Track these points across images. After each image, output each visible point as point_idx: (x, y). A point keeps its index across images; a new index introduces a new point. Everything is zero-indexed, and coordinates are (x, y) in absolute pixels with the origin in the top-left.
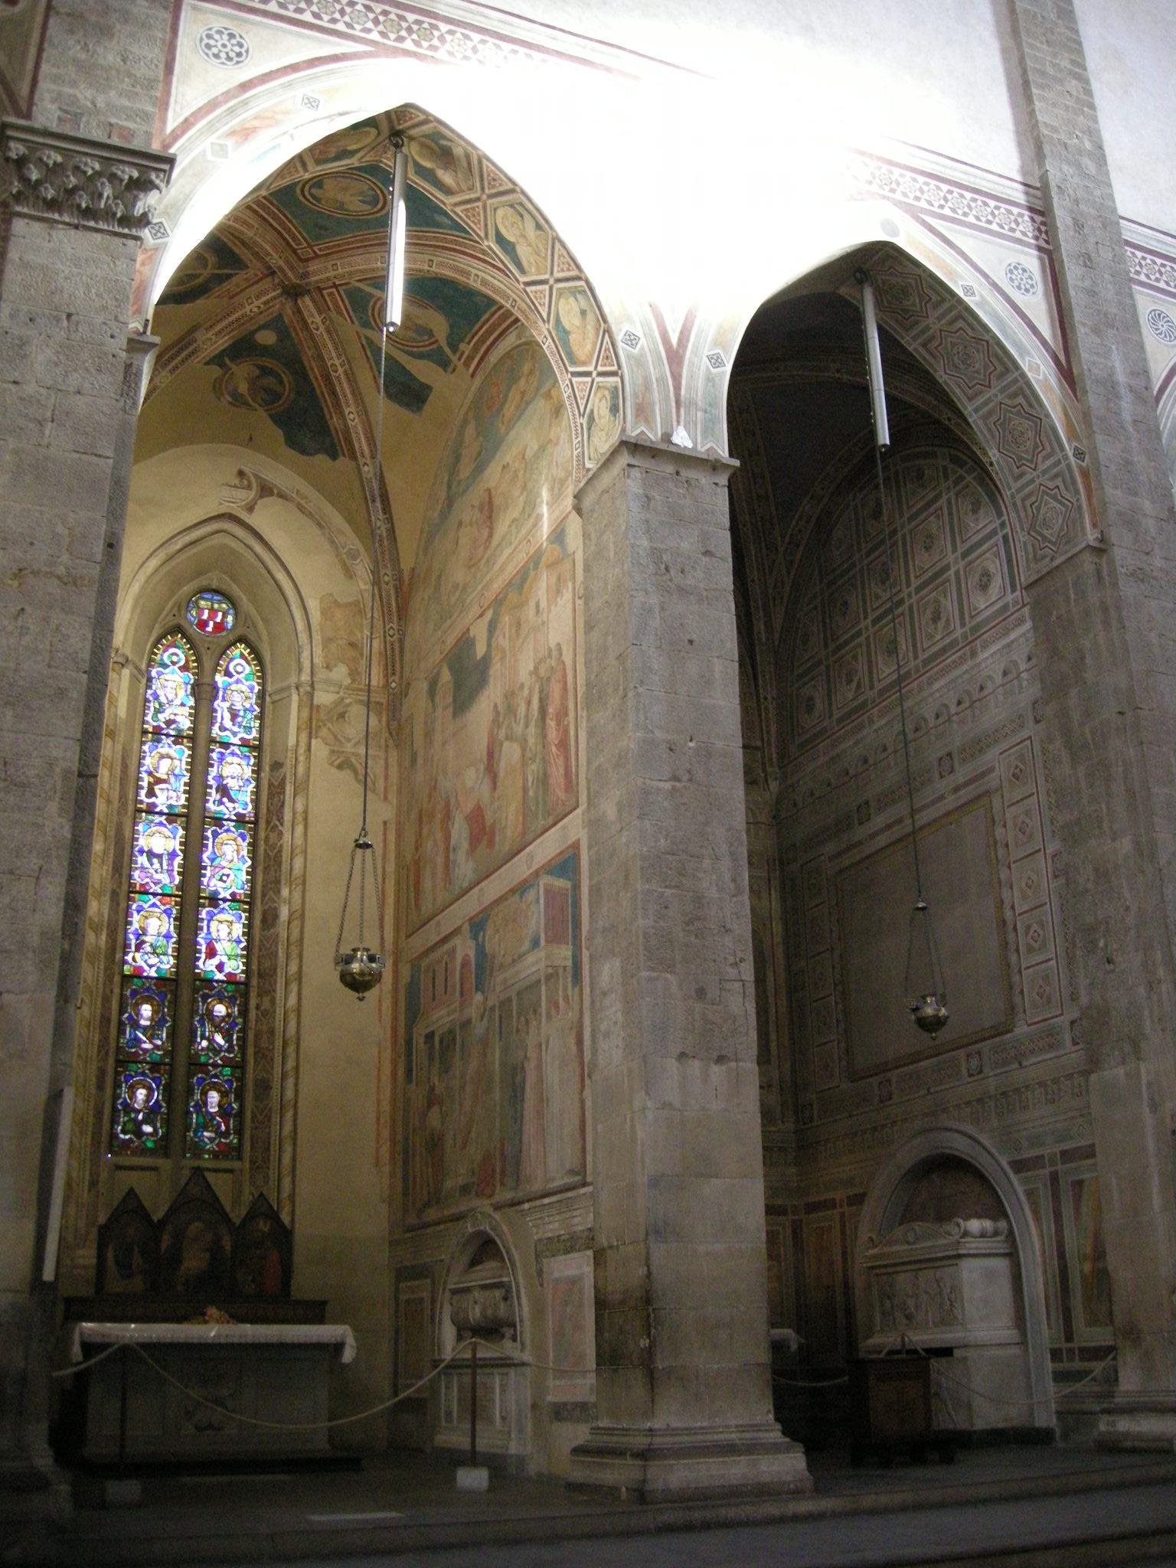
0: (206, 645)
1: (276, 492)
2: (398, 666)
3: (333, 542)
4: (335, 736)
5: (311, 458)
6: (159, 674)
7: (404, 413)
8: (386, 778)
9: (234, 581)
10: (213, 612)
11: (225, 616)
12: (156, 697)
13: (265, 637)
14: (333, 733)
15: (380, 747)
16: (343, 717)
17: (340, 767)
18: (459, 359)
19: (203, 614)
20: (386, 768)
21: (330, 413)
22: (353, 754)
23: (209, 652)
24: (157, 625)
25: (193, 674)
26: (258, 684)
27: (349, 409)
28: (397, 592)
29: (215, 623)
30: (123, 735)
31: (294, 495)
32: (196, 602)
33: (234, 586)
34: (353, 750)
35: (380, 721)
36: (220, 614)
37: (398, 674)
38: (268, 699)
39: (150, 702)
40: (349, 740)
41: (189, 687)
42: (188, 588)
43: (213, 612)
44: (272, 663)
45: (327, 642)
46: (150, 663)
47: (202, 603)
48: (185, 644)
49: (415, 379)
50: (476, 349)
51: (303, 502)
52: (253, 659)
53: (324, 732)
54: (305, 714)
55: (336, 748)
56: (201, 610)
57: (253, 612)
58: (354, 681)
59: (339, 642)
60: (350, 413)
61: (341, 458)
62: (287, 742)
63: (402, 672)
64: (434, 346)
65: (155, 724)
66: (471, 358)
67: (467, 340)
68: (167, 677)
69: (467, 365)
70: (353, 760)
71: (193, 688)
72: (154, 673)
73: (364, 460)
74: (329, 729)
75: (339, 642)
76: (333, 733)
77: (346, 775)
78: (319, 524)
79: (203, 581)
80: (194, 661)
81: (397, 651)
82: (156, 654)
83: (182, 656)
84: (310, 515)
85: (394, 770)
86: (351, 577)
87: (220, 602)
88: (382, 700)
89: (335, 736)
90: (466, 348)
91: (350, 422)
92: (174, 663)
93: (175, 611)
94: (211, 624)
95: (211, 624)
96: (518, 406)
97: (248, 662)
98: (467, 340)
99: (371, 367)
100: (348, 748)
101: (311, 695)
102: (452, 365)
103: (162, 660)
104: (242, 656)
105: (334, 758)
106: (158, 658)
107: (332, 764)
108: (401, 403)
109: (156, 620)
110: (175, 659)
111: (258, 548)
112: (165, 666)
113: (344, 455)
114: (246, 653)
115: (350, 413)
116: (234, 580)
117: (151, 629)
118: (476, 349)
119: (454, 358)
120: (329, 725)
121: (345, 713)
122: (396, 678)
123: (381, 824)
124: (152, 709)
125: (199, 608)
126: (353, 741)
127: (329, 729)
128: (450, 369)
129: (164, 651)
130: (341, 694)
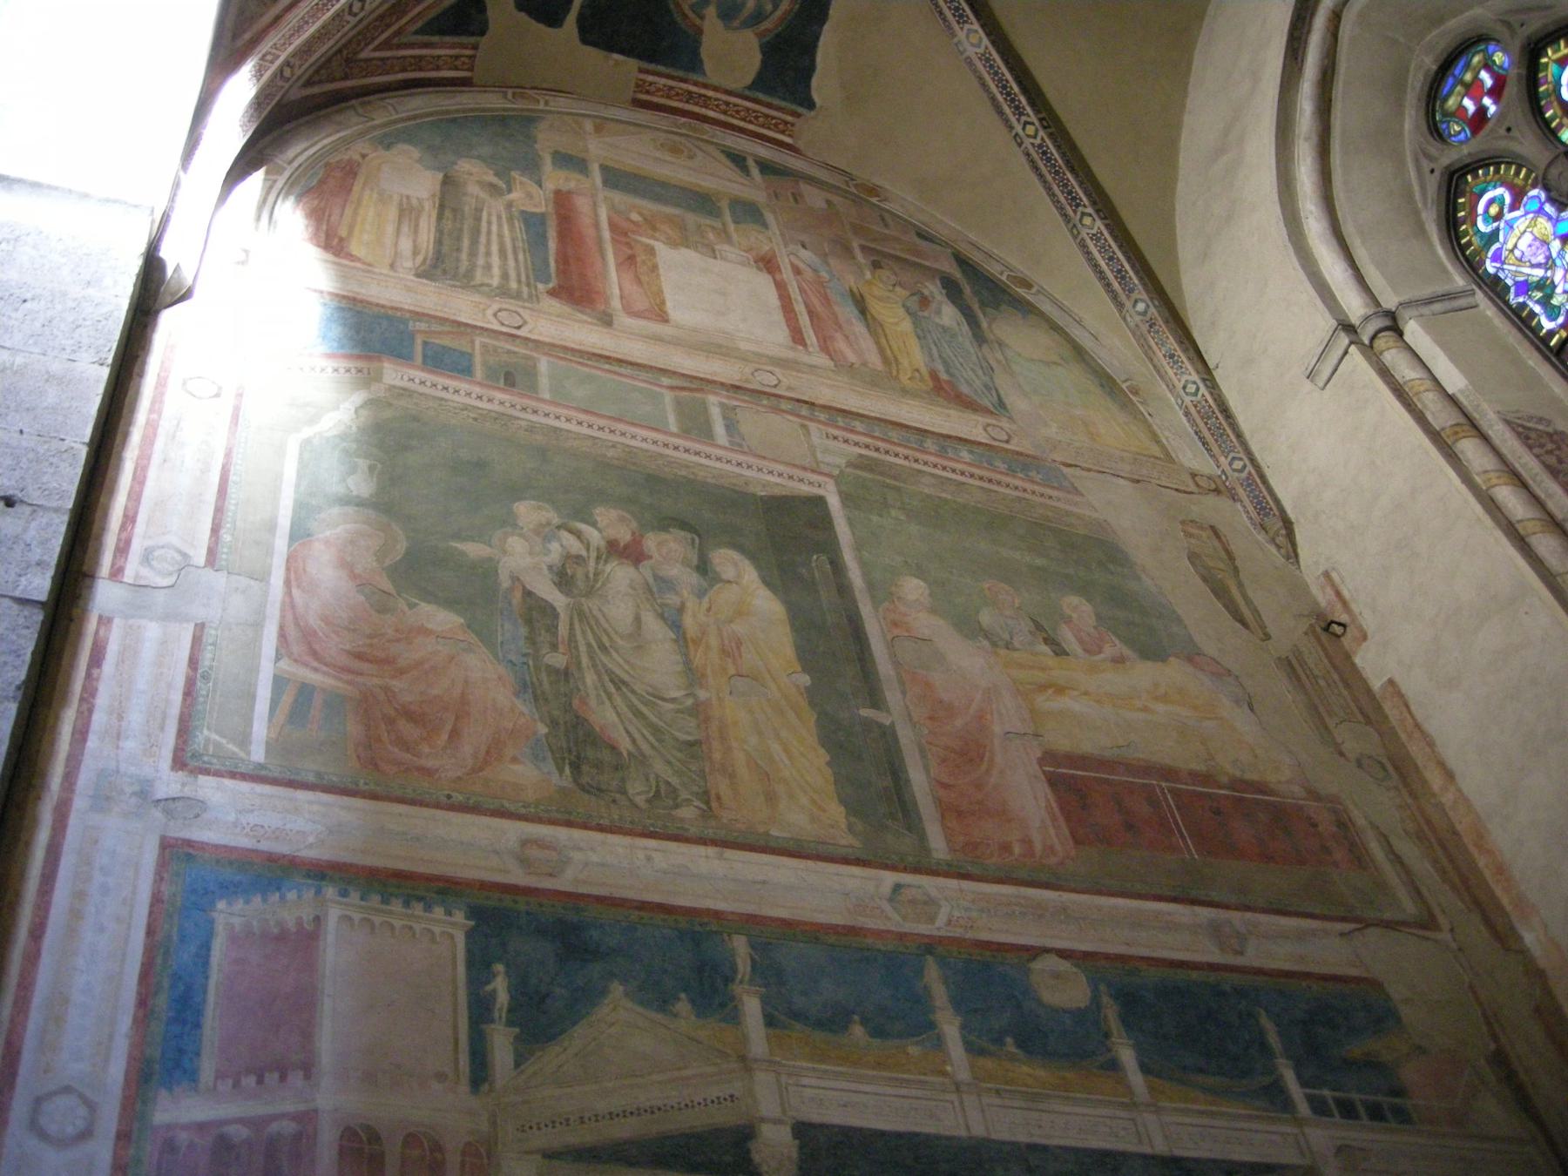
0: (1502, 132)
6: (1497, 257)
9: (1441, 20)
11: (1488, 66)
12: (1524, 287)
19: (1465, 109)
23: (1515, 133)
24: (1424, 215)
25: (1534, 186)
30: (1485, 406)
32: (1446, 114)
33: (1452, 23)
36: (1485, 76)
39: (1524, 305)
41: (1548, 208)
42: (1411, 120)
43: (1473, 89)
46: (1472, 265)
47: (1451, 103)
48: (1486, 174)
65: (1561, 320)
68: (1510, 246)
71: (1550, 200)
72: (1490, 267)
79: (1416, 83)
80: (1517, 173)
82: (1469, 244)
83: (1500, 191)
87: (1467, 66)
92: (1499, 217)
93: (1426, 165)
94: (1487, 101)
95: (1487, 101)
103: (1482, 235)
106: (1476, 241)
109: (1417, 213)
110: (1494, 210)
112: (1494, 235)
116: (1437, 20)
117: (1421, 230)
124: (1537, 309)
129: (1474, 224)
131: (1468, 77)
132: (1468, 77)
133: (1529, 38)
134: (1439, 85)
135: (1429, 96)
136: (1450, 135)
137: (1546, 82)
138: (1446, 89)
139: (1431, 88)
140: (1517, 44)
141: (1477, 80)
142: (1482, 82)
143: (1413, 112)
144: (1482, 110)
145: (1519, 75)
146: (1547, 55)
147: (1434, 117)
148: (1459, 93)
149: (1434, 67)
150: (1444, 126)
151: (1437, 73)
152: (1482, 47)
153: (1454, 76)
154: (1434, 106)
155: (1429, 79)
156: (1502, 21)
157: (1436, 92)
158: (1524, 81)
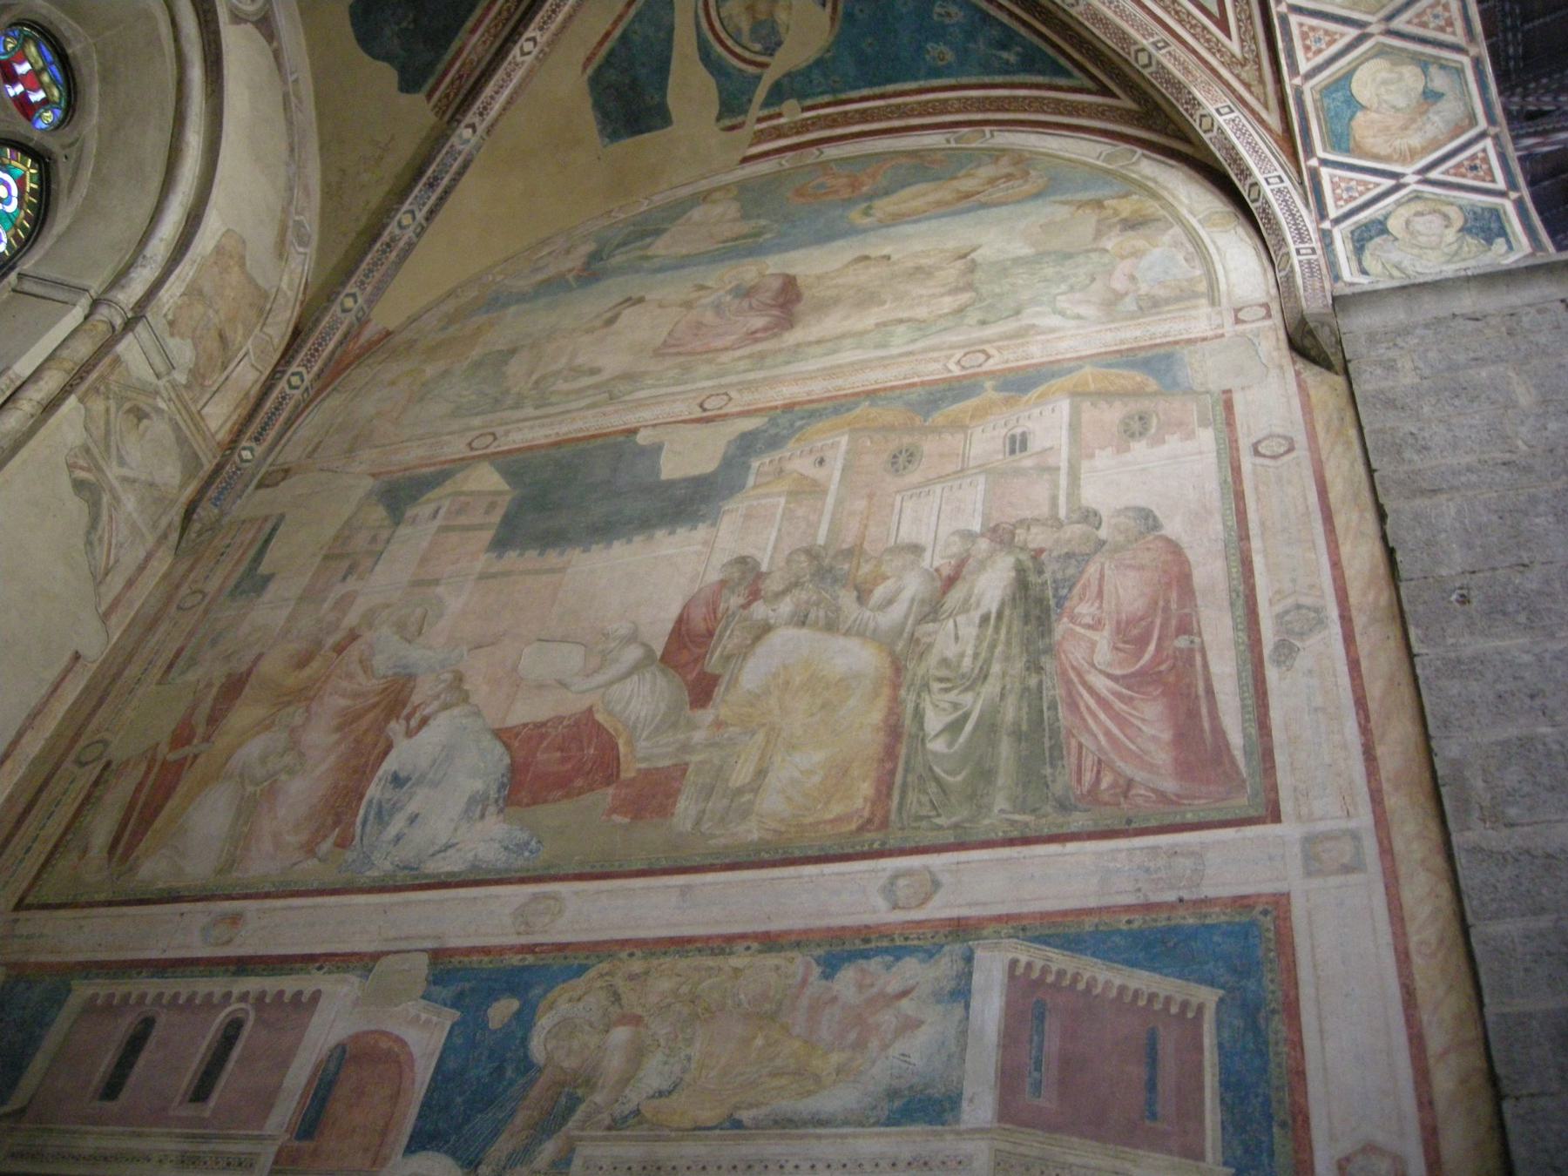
1: (275, 44)
2: (271, 435)
3: (291, 189)
4: (108, 433)
5: (367, 58)
7: (587, 119)
8: (130, 583)
10: (33, 80)
13: (82, 190)
14: (107, 423)
15: (155, 526)
16: (140, 419)
17: (79, 485)
18: (760, 120)
19: (21, 63)
20: (142, 568)
21: (480, 21)
22: (112, 490)
26: (9, 246)
27: (537, 34)
28: (346, 336)
29: (24, 95)
31: (291, 79)
32: (26, 38)
33: (96, 87)
34: (116, 484)
35: (183, 486)
37: (265, 445)
38: (13, 277)
40: (122, 462)
43: (33, 80)
44: (60, 238)
45: (194, 292)
47: (32, 50)
49: (662, 87)
50: (803, 127)
51: (293, 99)
52: (30, 205)
53: (98, 405)
54: (83, 349)
55: (95, 451)
56: (23, 58)
57: (92, 147)
58: (188, 386)
59: (211, 313)
60: (534, 39)
61: (420, 97)
62: (17, 357)
63: (271, 449)
64: (751, 69)
66: (779, 133)
67: (809, 102)
69: (760, 137)
70: (106, 498)
73: (477, 120)
74: (107, 410)
75: (211, 313)
76: (107, 423)
77: (76, 507)
78: (292, 150)
81: (284, 415)
84: (290, 122)
85: (150, 582)
86: (281, 256)
87: (54, 81)
88: (204, 460)
89: (108, 433)
90: (791, 112)
91: (516, 51)
94: (19, 89)
95: (19, 89)
96: (939, 204)
97: (20, 198)
98: (809, 102)
99: (620, 17)
100: (113, 472)
101: (114, 337)
102: (740, 119)
104: (21, 182)
105: (81, 462)
107: (71, 467)
108: (598, 106)
111: (196, 74)
113: (429, 96)
114: (30, 185)
115: (534, 39)
118: (803, 127)
119: (755, 111)
120: (112, 403)
121: (146, 416)
122: (260, 449)
123: (67, 657)
125: (22, 47)
126: (125, 472)
127: (107, 410)
128: (727, 122)
130: (161, 383)
131: (46, 78)
132: (46, 78)
133: (55, 162)
134: (53, 46)
135: (48, 31)
136: (7, 35)
137: (12, 158)
138: (44, 48)
139: (53, 36)
140: (53, 144)
141: (41, 86)
142: (35, 91)
143: (44, 11)
144: (13, 79)
145: (32, 140)
146: (32, 167)
147: (28, 26)
148: (37, 62)
149: (69, 51)
150: (16, 33)
151: (63, 50)
152: (63, 105)
153: (51, 63)
154: (39, 32)
155: (62, 40)
156: (77, 140)
157: (47, 39)
158: (24, 141)
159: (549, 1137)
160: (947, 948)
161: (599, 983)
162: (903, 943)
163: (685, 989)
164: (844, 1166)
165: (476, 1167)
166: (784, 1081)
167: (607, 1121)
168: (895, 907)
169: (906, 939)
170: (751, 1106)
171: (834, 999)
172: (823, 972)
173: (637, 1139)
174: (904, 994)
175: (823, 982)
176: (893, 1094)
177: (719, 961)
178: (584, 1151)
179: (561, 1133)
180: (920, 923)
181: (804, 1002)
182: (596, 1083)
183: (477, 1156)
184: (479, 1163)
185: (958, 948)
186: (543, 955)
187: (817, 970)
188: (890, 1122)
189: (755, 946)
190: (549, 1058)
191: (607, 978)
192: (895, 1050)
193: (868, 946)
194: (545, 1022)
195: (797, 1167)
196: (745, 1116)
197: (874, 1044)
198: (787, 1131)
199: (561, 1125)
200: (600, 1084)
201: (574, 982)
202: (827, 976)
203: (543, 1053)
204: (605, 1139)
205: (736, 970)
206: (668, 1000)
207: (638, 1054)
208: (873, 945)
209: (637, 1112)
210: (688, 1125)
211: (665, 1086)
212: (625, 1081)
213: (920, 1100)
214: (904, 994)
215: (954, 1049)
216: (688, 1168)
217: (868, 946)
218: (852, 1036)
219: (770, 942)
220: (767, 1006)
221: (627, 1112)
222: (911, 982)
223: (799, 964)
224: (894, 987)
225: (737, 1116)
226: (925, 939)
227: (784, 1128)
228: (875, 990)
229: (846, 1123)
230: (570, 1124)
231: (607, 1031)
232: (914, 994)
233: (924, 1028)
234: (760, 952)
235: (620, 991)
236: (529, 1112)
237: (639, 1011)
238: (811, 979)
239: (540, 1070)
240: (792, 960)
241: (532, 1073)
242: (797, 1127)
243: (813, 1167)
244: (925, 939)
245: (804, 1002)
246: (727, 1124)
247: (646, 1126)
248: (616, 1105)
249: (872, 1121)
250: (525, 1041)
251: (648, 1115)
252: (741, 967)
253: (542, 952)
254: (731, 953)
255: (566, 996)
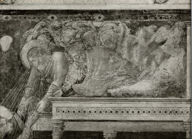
159: (41, 99)
160: (177, 23)
161: (42, 31)
162: (160, 20)
163: (78, 36)
164: (149, 112)
165: (16, 112)
166: (123, 78)
167: (61, 93)
168: (155, 2)
169: (161, 18)
170: (113, 88)
171: (137, 44)
172: (131, 31)
173: (74, 100)
174: (163, 43)
175: (132, 36)
176: (163, 85)
177: (89, 23)
178: (55, 105)
179: (45, 98)
180: (165, 11)
181: (125, 44)
182: (53, 77)
183: (15, 106)
184: (17, 110)
185: (181, 23)
186: (15, 16)
187: (128, 30)
188: (163, 96)
189: (102, 16)
190: (31, 66)
191: (46, 29)
192: (161, 67)
193: (146, 20)
194: (25, 49)
195: (133, 112)
196: (112, 91)
197: (153, 63)
198: (128, 98)
199: (44, 94)
200: (54, 77)
201: (32, 30)
202: (133, 33)
203: (29, 63)
204: (62, 100)
205: (97, 28)
206: (72, 41)
207: (66, 64)
208: (148, 20)
209: (72, 89)
210: (91, 94)
211: (79, 79)
212: (64, 76)
213: (172, 88)
214: (163, 43)
215: (182, 67)
216: (95, 112)
217: (146, 20)
218: (145, 60)
219: (108, 15)
220: (112, 45)
221: (68, 89)
222: (165, 38)
223: (122, 26)
224: (158, 40)
225: (109, 91)
226: (168, 18)
227: (126, 97)
228: (151, 40)
229: (148, 96)
230: (47, 94)
231: (52, 54)
232: (166, 43)
233: (171, 58)
234: (105, 20)
235: (52, 35)
236: (30, 89)
237: (61, 45)
238: (127, 34)
239: (30, 70)
240: (118, 24)
241: (27, 72)
242: (131, 97)
243: (138, 112)
244: (168, 18)
245: (125, 44)
246: (106, 95)
247: (76, 95)
248: (63, 86)
249: (157, 95)
250: (19, 57)
251: (76, 91)
252: (99, 26)
253: (14, 14)
254: (94, 20)
255: (30, 37)
